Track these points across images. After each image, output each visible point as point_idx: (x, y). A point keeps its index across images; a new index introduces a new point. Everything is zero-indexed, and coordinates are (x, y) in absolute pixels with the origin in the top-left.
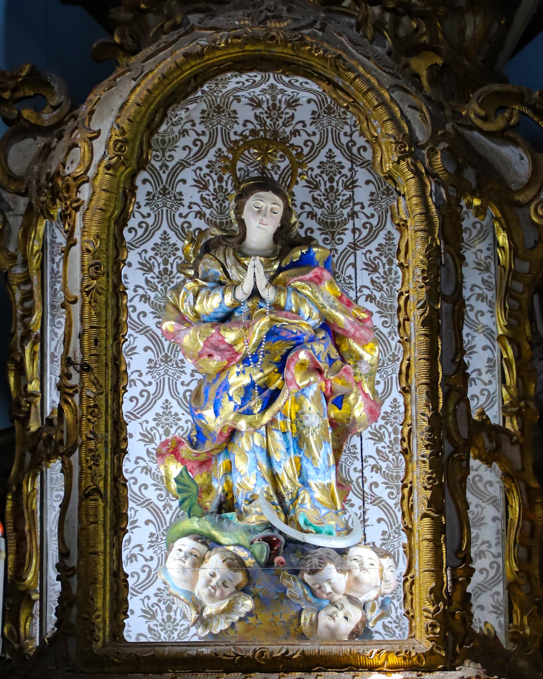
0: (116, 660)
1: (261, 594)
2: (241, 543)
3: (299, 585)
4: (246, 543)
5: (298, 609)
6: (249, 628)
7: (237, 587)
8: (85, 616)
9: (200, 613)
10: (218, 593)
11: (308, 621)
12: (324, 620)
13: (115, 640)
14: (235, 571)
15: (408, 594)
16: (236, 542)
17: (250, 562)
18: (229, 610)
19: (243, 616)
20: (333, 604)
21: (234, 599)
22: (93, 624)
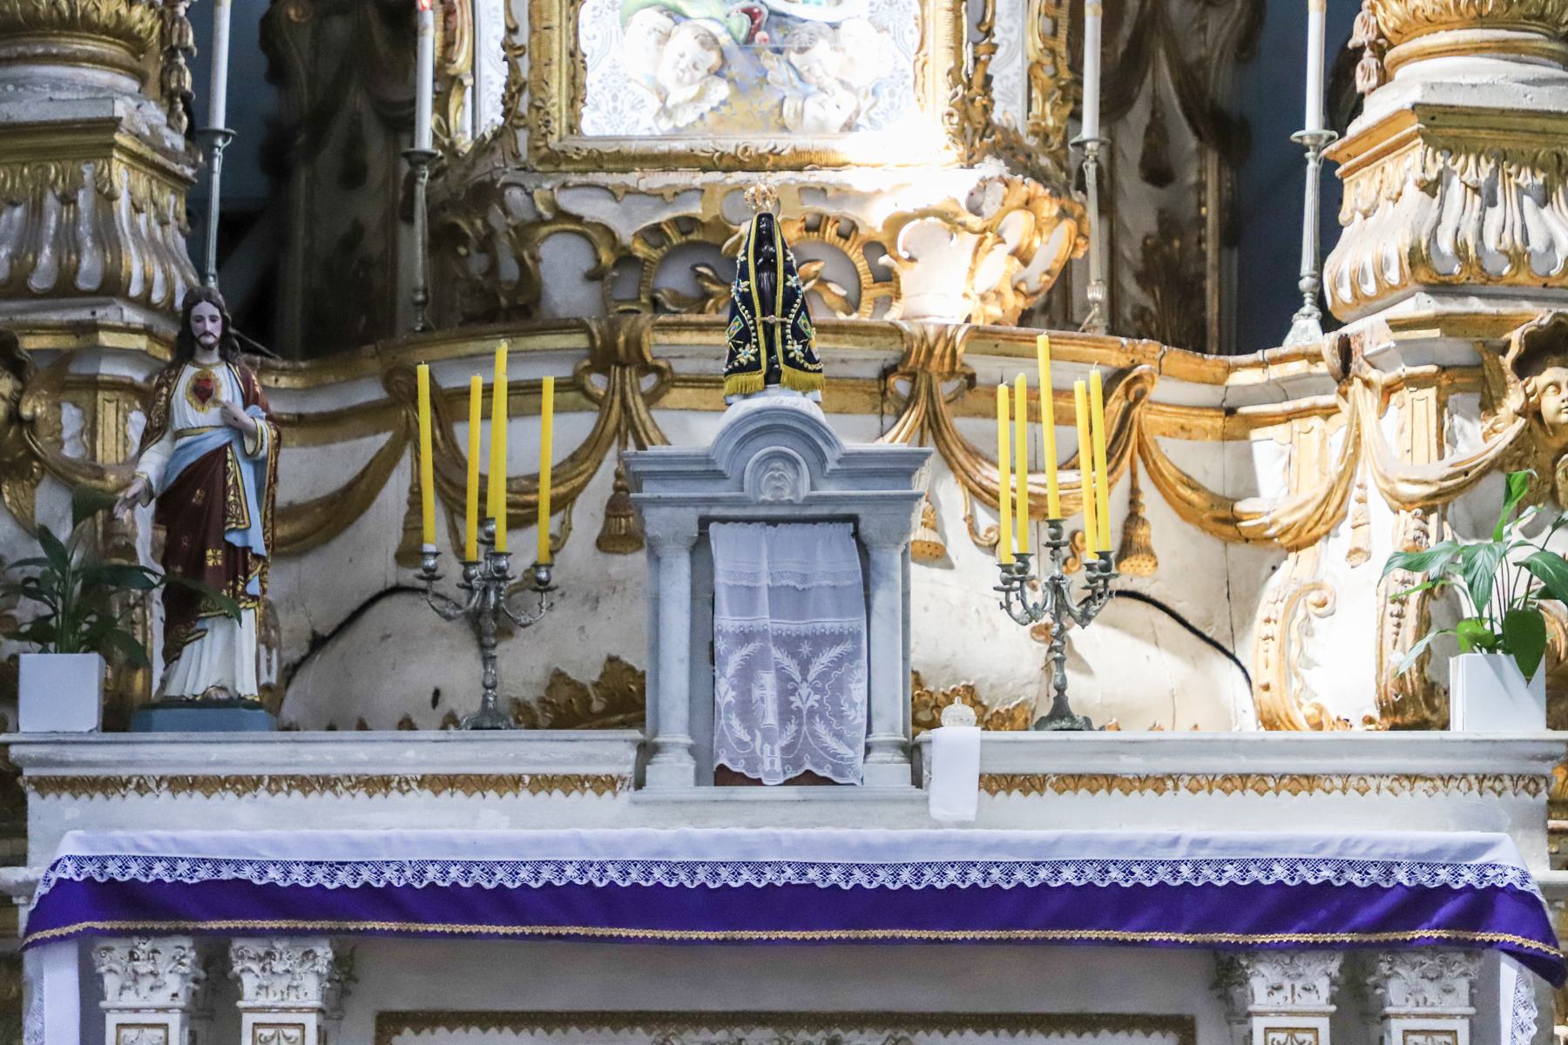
0: (575, 157)
1: (737, 79)
2: (714, 16)
3: (784, 66)
4: (721, 17)
5: (781, 96)
6: (721, 120)
7: (709, 70)
8: (538, 103)
9: (664, 102)
10: (687, 77)
11: (792, 112)
12: (811, 108)
13: (572, 132)
14: (709, 50)
15: (920, 76)
16: (708, 14)
17: (724, 39)
18: (699, 97)
19: (715, 104)
20: (822, 90)
21: (706, 84)
22: (548, 113)
